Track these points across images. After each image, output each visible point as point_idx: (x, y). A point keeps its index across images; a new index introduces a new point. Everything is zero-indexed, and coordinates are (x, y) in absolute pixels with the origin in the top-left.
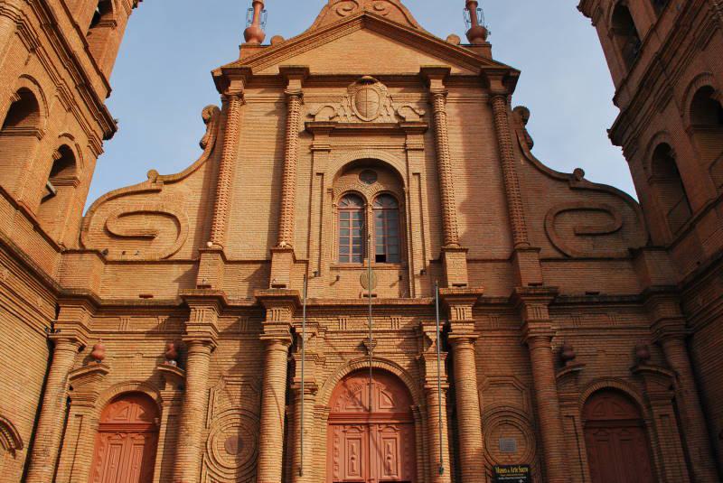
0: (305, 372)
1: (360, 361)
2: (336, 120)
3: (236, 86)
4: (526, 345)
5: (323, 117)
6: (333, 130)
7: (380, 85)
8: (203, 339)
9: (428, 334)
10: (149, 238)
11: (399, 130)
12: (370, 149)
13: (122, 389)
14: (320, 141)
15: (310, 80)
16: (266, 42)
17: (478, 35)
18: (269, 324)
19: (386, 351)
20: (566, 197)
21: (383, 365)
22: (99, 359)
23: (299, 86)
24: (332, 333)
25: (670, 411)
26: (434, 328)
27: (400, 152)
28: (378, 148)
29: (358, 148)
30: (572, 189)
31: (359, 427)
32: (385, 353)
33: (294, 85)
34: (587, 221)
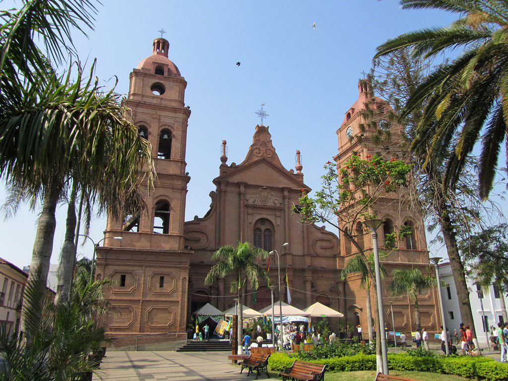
2: (255, 203)
3: (223, 187)
4: (305, 282)
5: (251, 202)
6: (255, 207)
7: (269, 190)
10: (198, 240)
11: (274, 209)
12: (265, 215)
13: (197, 290)
14: (250, 211)
15: (247, 186)
17: (300, 168)
20: (319, 235)
22: (191, 281)
27: (274, 217)
29: (261, 214)
30: (322, 233)
33: (242, 189)
34: (324, 244)
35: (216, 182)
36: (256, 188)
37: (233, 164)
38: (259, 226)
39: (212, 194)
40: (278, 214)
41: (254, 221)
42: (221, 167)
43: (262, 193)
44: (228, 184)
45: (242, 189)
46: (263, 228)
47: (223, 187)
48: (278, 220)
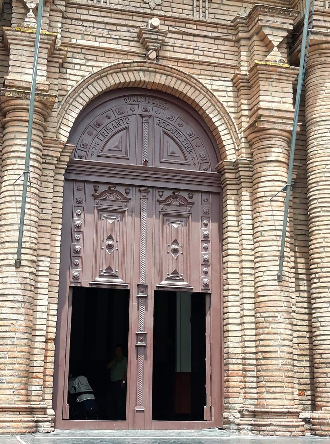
9: (267, 31)
19: (180, 56)
21: (172, 83)
26: (279, 21)
31: (122, 190)
32: (178, 60)
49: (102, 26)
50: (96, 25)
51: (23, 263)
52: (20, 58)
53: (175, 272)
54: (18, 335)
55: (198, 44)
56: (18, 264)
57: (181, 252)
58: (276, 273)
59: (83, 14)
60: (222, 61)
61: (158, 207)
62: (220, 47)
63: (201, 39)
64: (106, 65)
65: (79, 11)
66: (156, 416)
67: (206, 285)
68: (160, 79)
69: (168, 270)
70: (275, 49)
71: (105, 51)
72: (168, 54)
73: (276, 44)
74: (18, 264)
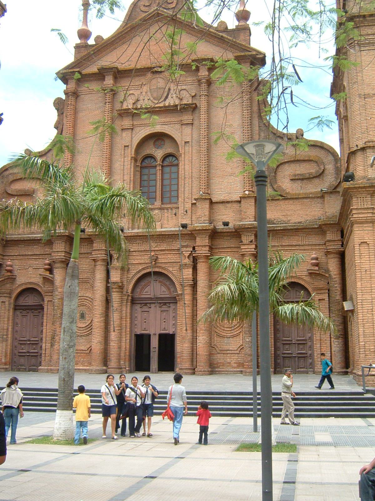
0: (115, 277)
1: (147, 268)
5: (129, 104)
8: (60, 260)
9: (184, 253)
10: (28, 194)
13: (24, 287)
14: (127, 122)
16: (91, 42)
18: (95, 250)
19: (163, 261)
21: (161, 270)
23: (111, 82)
24: (133, 252)
25: (326, 297)
27: (178, 126)
28: (164, 124)
35: (64, 76)
36: (141, 75)
37: (98, 38)
38: (150, 149)
39: (59, 104)
40: (187, 118)
41: (136, 141)
42: (78, 47)
43: (154, 81)
44: (85, 78)
45: (109, 81)
46: (159, 154)
47: (72, 85)
48: (187, 130)
49: (140, 256)
50: (138, 256)
51: (115, 330)
52: (113, 274)
53: (164, 328)
54: (115, 349)
55: (169, 256)
56: (114, 331)
57: (166, 322)
58: (185, 328)
59: (134, 254)
60: (176, 261)
61: (159, 309)
62: (176, 256)
63: (169, 255)
64: (141, 268)
65: (133, 253)
66: (159, 371)
67: (174, 332)
68: (157, 270)
69: (163, 327)
70: (187, 258)
71: (140, 264)
72: (161, 261)
73: (187, 256)
74: (114, 331)
